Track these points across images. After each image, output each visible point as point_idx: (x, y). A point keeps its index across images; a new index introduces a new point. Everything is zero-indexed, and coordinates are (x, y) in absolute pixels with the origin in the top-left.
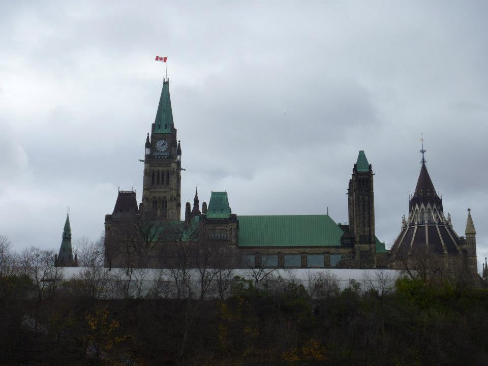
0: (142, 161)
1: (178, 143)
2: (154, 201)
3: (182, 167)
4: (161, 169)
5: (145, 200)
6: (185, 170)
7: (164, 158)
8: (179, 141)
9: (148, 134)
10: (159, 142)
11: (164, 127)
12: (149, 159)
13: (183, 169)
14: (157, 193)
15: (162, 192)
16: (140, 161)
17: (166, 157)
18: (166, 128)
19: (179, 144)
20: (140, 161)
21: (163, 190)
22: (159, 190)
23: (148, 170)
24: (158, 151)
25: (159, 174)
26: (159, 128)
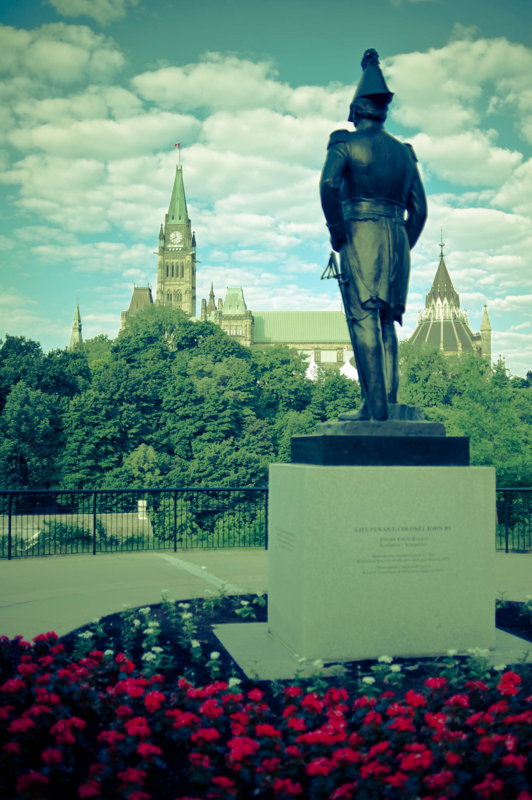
0: (157, 254)
1: (192, 234)
2: (168, 294)
4: (175, 261)
6: (200, 262)
7: (178, 250)
8: (194, 233)
9: (162, 225)
10: (173, 234)
11: (178, 218)
15: (176, 285)
17: (180, 249)
19: (194, 236)
21: (178, 283)
22: (173, 283)
25: (173, 267)
26: (173, 219)
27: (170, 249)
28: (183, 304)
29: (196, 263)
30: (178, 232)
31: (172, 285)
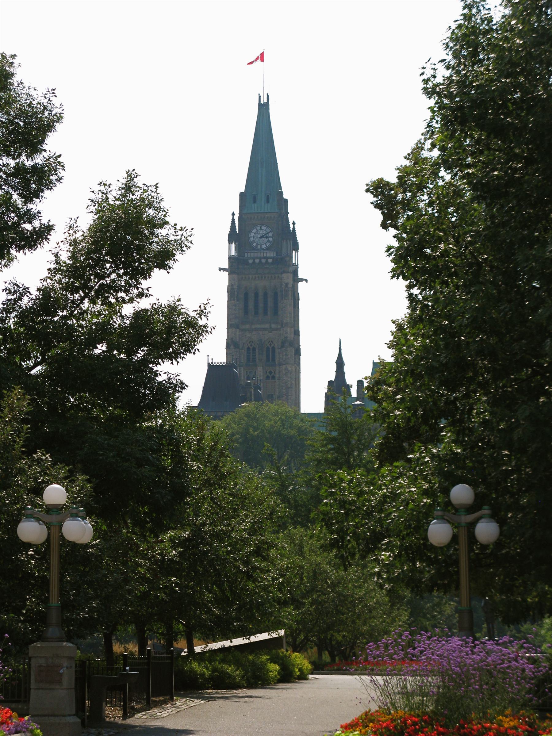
0: (224, 270)
1: (291, 226)
2: (248, 349)
3: (300, 276)
5: (232, 347)
7: (267, 262)
8: (294, 223)
9: (233, 214)
12: (236, 267)
13: (302, 280)
14: (254, 333)
15: (264, 329)
16: (220, 269)
17: (270, 261)
18: (268, 201)
19: (294, 228)
20: (220, 269)
21: (267, 326)
22: (258, 326)
23: (235, 287)
24: (254, 249)
26: (255, 202)
27: (251, 261)
28: (278, 368)
29: (300, 283)
30: (264, 228)
31: (256, 330)
